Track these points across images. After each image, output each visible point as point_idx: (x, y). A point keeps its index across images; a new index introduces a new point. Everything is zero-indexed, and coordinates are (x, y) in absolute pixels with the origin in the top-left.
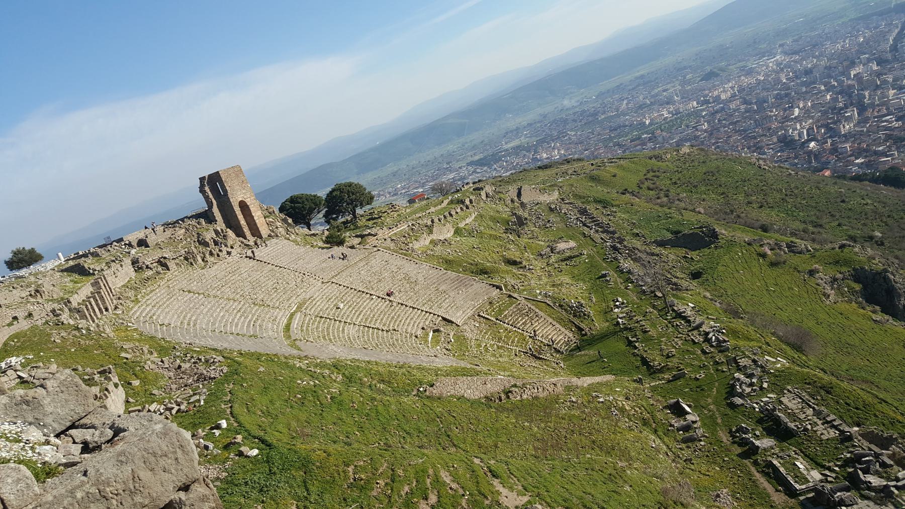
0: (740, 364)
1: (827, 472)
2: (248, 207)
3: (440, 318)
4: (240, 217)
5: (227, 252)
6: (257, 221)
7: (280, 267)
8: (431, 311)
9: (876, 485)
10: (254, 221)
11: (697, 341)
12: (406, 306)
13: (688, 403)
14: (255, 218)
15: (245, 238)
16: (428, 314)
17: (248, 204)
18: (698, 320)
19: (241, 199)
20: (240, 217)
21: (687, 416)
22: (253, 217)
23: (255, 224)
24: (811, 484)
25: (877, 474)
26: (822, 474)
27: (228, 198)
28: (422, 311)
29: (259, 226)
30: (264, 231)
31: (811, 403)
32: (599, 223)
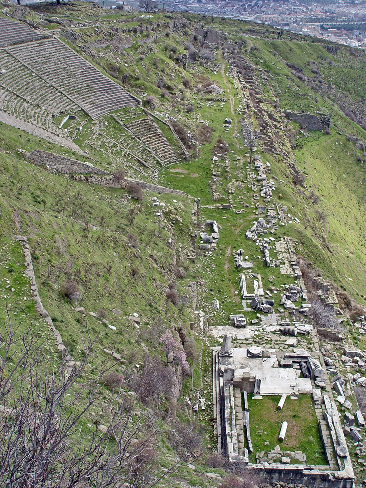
0: (268, 213)
1: (268, 292)
3: (80, 109)
8: (75, 100)
9: (288, 306)
11: (253, 189)
12: (57, 90)
13: (219, 226)
16: (72, 102)
18: (264, 176)
21: (213, 234)
24: (254, 295)
25: (295, 301)
26: (264, 292)
28: (68, 98)
31: (290, 251)
32: (252, 82)
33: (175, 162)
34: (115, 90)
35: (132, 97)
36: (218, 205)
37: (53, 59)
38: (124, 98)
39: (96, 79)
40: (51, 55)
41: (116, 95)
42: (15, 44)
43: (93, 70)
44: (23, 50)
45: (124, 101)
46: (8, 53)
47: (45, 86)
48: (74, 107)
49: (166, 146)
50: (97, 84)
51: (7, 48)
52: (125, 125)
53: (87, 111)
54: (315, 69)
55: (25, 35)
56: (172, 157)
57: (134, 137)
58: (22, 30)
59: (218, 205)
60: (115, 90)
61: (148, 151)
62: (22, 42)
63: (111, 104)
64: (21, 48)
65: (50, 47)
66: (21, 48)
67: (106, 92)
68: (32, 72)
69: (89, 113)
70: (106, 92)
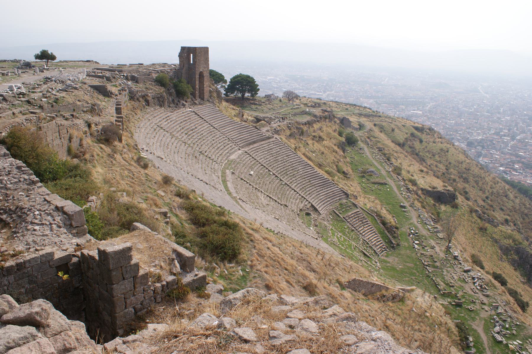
2: (203, 77)
4: (197, 82)
5: (183, 104)
6: (205, 88)
7: (214, 128)
10: (204, 87)
14: (205, 86)
15: (195, 97)
17: (204, 75)
19: (201, 70)
20: (197, 82)
22: (204, 84)
23: (203, 90)
27: (195, 67)
29: (205, 92)
30: (206, 95)
33: (386, 250)
34: (329, 185)
35: (342, 191)
36: (449, 300)
37: (279, 158)
38: (337, 192)
39: (314, 175)
40: (278, 153)
41: (331, 189)
42: (250, 144)
43: (309, 166)
44: (257, 150)
45: (337, 195)
46: (248, 154)
47: (281, 184)
48: (306, 204)
49: (377, 236)
50: (316, 179)
51: (246, 150)
52: (344, 218)
53: (315, 206)
54: (411, 145)
55: (255, 136)
56: (383, 246)
57: (353, 229)
58: (253, 132)
59: (449, 300)
60: (329, 185)
61: (366, 241)
62: (254, 142)
63: (329, 198)
64: (255, 149)
65: (275, 146)
66: (255, 149)
67: (324, 187)
68: (269, 171)
69: (317, 207)
70: (324, 187)
